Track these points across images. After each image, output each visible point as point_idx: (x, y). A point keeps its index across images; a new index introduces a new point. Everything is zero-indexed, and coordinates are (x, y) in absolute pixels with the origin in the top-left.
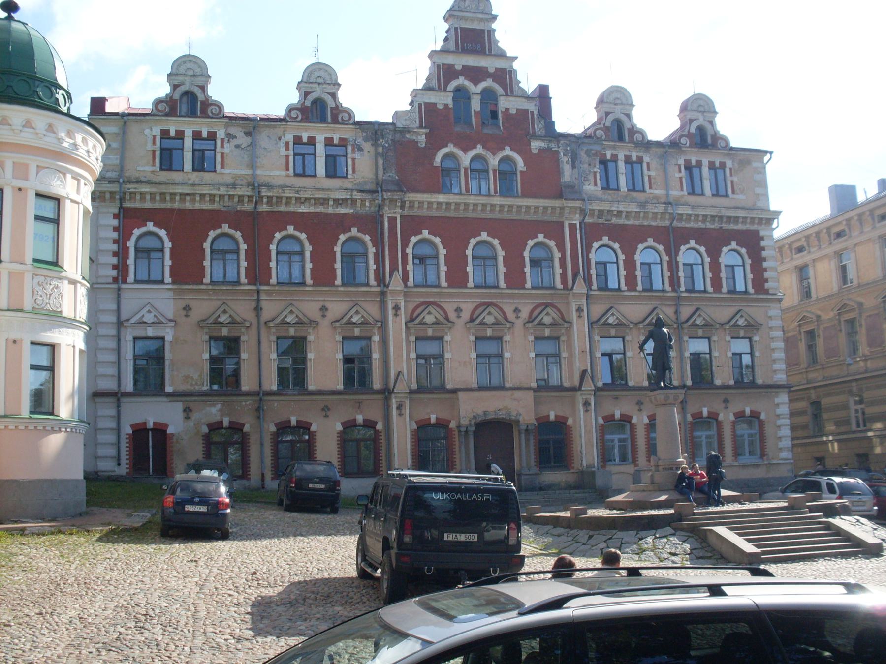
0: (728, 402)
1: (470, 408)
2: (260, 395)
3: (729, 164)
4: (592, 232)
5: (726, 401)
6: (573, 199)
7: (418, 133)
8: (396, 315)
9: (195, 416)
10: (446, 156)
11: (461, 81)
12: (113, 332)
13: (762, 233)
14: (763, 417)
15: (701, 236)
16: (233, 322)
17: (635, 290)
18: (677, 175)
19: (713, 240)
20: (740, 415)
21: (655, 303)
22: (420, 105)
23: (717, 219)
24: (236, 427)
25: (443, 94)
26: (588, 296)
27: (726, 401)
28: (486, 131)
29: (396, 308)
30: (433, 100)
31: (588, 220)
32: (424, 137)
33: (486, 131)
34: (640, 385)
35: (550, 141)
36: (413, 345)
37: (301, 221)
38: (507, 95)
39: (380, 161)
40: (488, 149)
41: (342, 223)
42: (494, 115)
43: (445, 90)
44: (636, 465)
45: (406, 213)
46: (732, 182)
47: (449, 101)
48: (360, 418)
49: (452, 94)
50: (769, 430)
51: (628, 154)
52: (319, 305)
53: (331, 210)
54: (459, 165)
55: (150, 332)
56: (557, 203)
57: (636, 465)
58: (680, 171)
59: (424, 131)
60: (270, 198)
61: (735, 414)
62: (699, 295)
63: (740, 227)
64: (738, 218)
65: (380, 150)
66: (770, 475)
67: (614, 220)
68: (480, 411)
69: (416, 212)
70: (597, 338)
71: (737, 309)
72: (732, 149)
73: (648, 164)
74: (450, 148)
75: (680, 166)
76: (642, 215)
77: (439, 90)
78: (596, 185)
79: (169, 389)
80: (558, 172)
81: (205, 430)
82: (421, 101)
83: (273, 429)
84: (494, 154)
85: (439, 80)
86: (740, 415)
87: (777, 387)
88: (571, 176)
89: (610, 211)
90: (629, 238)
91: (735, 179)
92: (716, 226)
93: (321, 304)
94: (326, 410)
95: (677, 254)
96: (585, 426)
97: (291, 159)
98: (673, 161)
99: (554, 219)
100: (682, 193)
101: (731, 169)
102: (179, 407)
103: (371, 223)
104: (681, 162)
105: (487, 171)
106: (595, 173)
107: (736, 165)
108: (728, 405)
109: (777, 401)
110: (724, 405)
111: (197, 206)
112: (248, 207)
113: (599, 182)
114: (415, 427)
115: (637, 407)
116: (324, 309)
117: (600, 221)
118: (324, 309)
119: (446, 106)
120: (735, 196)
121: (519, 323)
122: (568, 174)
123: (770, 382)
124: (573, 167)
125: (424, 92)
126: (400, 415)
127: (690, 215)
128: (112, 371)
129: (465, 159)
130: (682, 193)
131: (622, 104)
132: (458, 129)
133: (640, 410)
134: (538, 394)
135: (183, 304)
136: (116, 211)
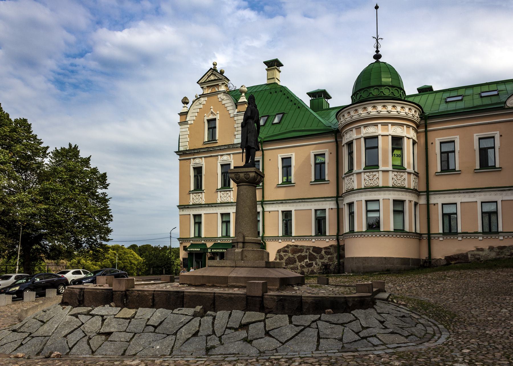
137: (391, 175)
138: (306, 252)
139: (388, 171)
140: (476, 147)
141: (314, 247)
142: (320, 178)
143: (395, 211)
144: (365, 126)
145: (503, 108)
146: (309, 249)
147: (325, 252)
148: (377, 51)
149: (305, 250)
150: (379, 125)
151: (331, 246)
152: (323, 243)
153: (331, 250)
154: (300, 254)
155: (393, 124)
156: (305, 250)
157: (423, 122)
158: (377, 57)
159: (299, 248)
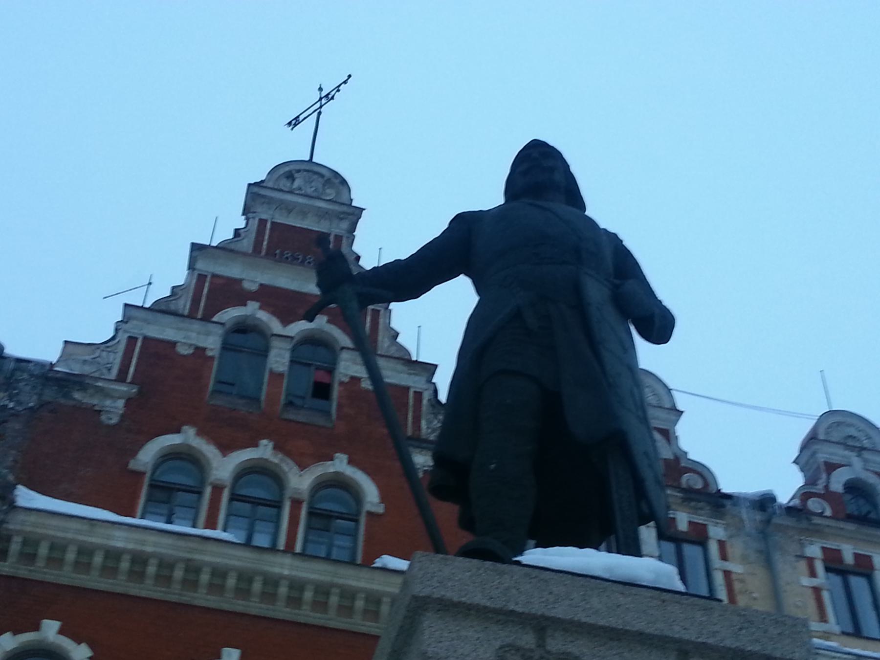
7: (104, 393)
10: (171, 456)
11: (252, 309)
22: (132, 340)
25: (196, 326)
28: (291, 415)
30: (169, 334)
32: (121, 403)
33: (291, 416)
40: (288, 454)
42: (322, 391)
43: (207, 318)
47: (211, 341)
49: (220, 330)
54: (203, 482)
59: (123, 388)
74: (188, 437)
77: (191, 316)
82: (135, 332)
84: (302, 466)
85: (196, 301)
105: (277, 505)
119: (200, 351)
125: (150, 316)
129: (224, 467)
132: (221, 401)
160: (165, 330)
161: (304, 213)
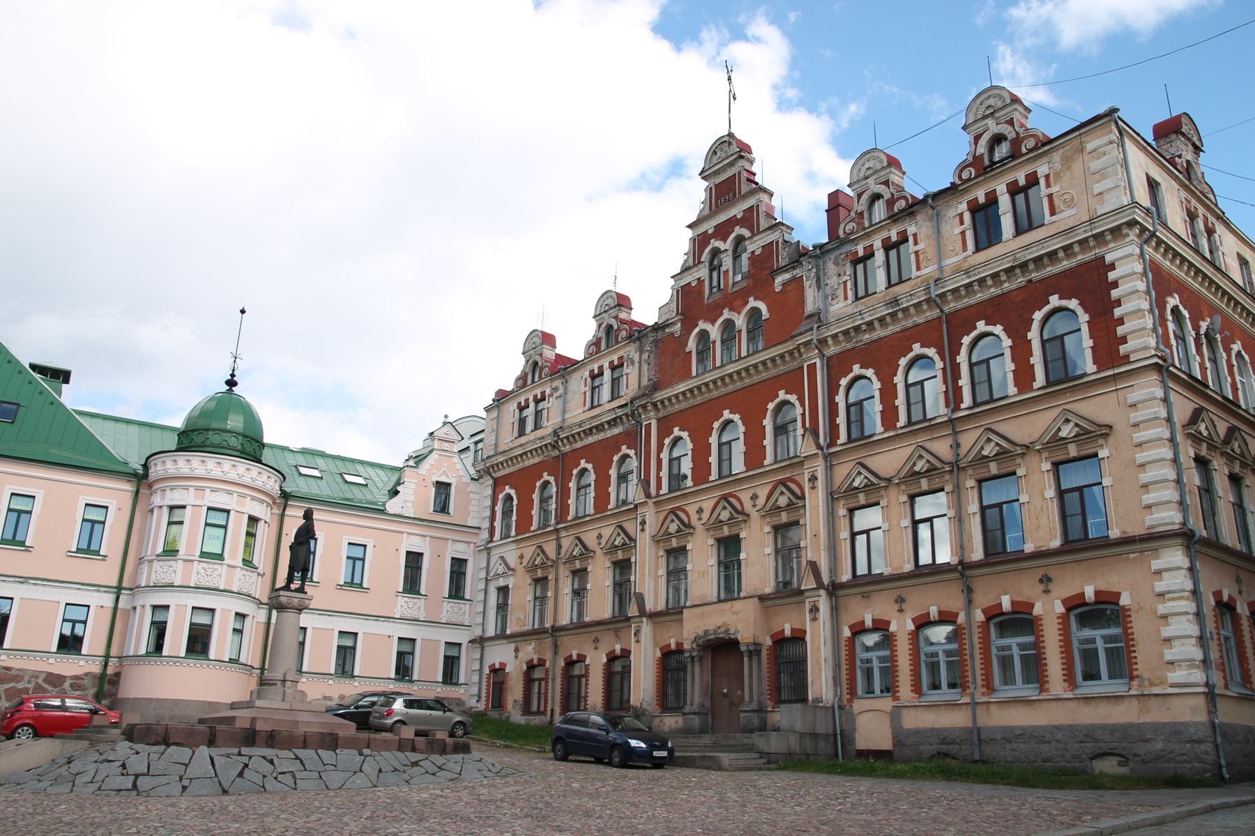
0: (1049, 580)
1: (693, 627)
2: (556, 630)
3: (1042, 169)
4: (836, 367)
5: (1046, 580)
6: (801, 334)
8: (643, 530)
9: (521, 654)
12: (482, 586)
13: (1109, 258)
14: (1125, 600)
15: (994, 310)
16: (543, 566)
17: (895, 428)
18: (958, 230)
19: (1012, 311)
20: (1074, 604)
21: (920, 439)
23: (1018, 271)
24: (542, 662)
26: (825, 457)
27: (1046, 580)
29: (643, 523)
31: (832, 350)
34: (899, 572)
35: (794, 268)
36: (663, 561)
37: (587, 452)
38: (753, 235)
39: (645, 367)
41: (612, 445)
43: (700, 262)
44: (896, 698)
45: (660, 415)
46: (1050, 196)
47: (703, 272)
48: (618, 648)
50: (1139, 626)
51: (884, 235)
52: (595, 533)
53: (609, 434)
55: (502, 582)
56: (789, 346)
57: (896, 698)
58: (962, 223)
60: (567, 438)
61: (1064, 602)
62: (987, 407)
63: (1066, 264)
64: (1055, 252)
65: (645, 356)
66: (1148, 718)
67: (867, 337)
68: (701, 633)
69: (670, 410)
70: (842, 512)
71: (1061, 408)
72: (1051, 141)
73: (915, 235)
74: (702, 325)
75: (961, 215)
76: (900, 315)
77: (695, 265)
78: (846, 298)
79: (508, 632)
80: (802, 302)
81: (525, 668)
83: (563, 664)
84: (739, 313)
86: (1074, 604)
87: (1153, 539)
88: (814, 302)
89: (857, 329)
90: (882, 357)
91: (1055, 189)
92: (1021, 280)
93: (598, 531)
94: (596, 640)
95: (955, 351)
96: (812, 641)
97: (589, 394)
98: (952, 213)
99: (795, 365)
100: (965, 254)
101: (1047, 177)
102: (513, 646)
103: (631, 438)
104: (963, 207)
106: (845, 283)
107: (1057, 165)
108: (1051, 586)
109: (1156, 564)
110: (1041, 587)
111: (532, 462)
112: (556, 453)
113: (850, 294)
114: (659, 654)
115: (897, 607)
116: (600, 537)
117: (849, 346)
118: (600, 537)
120: (1054, 218)
121: (754, 515)
122: (812, 300)
123: (1136, 530)
124: (819, 288)
126: (638, 641)
127: (970, 285)
128: (480, 620)
130: (965, 254)
131: (876, 172)
133: (901, 611)
134: (769, 603)
135: (519, 553)
136: (491, 482)
137: (239, 573)
138: (29, 682)
139: (235, 567)
140: (344, 554)
141: (49, 674)
142: (88, 550)
143: (235, 630)
144: (214, 490)
145: (383, 512)
146: (37, 677)
147: (71, 686)
148: (233, 375)
149: (27, 679)
150: (235, 495)
151: (86, 674)
152: (69, 666)
153: (86, 682)
154: (12, 684)
155: (253, 499)
156: (27, 679)
157: (283, 501)
158: (231, 383)
159: (13, 673)
160: (690, 278)
161: (723, 169)
